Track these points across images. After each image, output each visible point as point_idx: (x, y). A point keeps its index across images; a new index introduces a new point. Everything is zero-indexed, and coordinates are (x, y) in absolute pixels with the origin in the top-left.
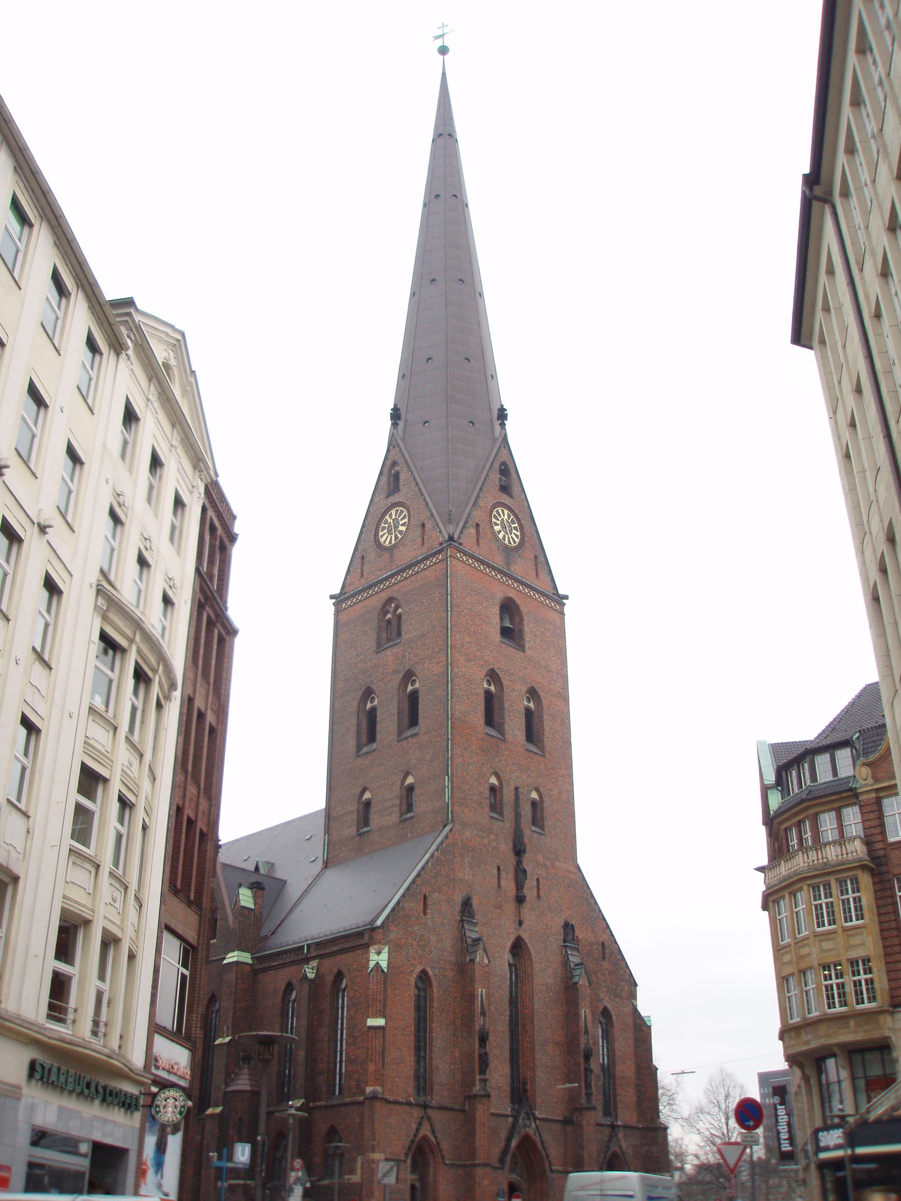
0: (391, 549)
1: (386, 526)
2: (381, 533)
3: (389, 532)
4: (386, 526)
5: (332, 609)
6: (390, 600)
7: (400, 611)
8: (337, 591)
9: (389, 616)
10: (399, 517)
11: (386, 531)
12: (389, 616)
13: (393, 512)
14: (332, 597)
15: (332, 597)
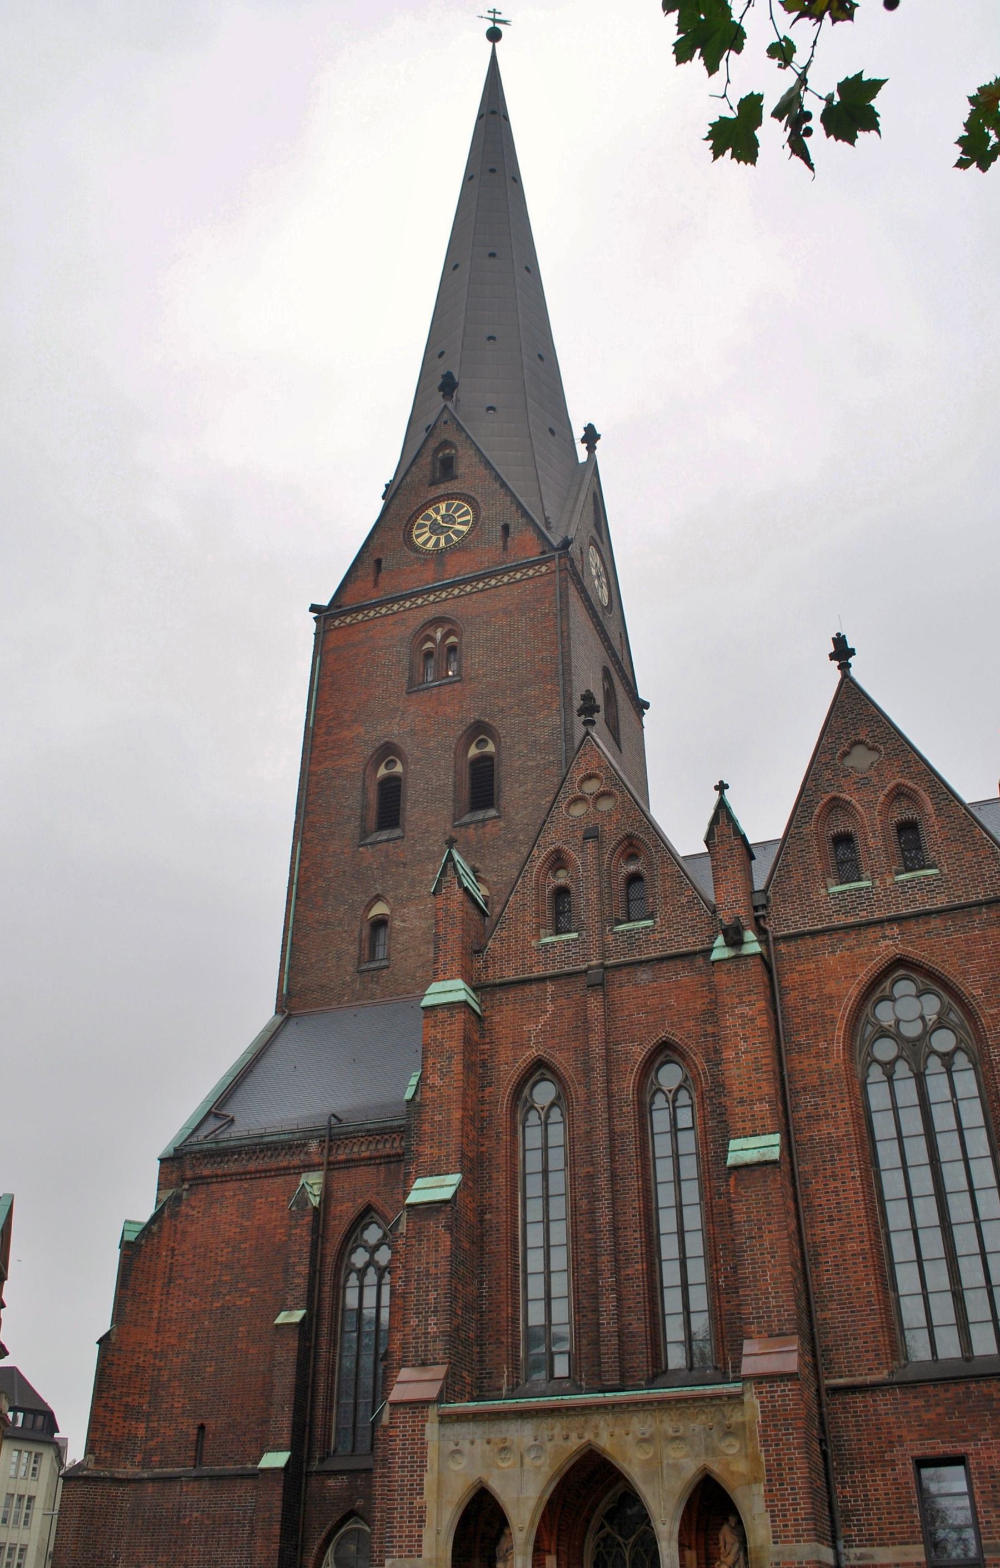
0: (439, 554)
1: (428, 523)
2: (415, 532)
3: (433, 531)
4: (428, 523)
5: (314, 625)
6: (437, 622)
7: (452, 639)
8: (325, 601)
9: (429, 645)
10: (455, 512)
11: (427, 529)
12: (429, 645)
13: (443, 507)
14: (314, 608)
15: (314, 608)
